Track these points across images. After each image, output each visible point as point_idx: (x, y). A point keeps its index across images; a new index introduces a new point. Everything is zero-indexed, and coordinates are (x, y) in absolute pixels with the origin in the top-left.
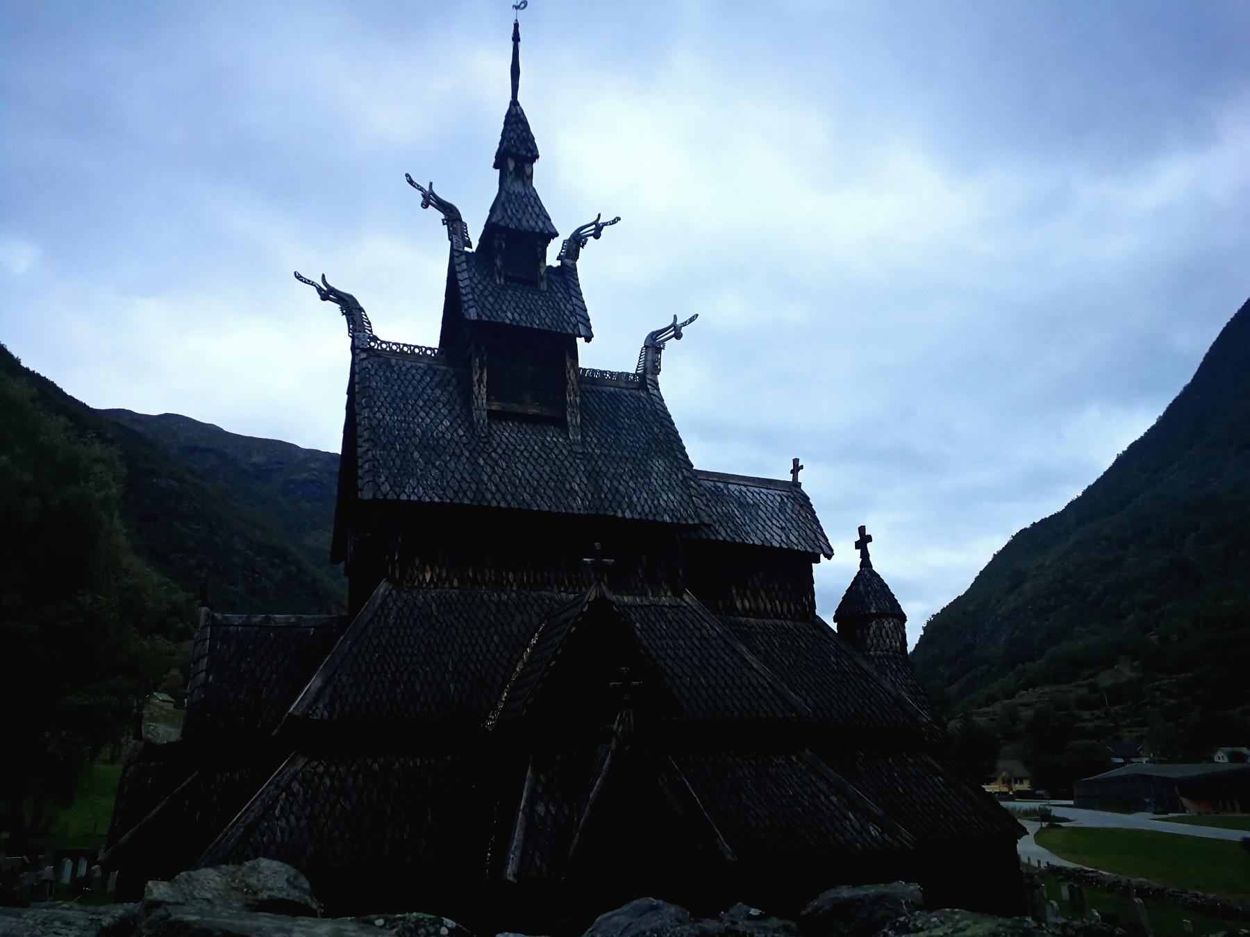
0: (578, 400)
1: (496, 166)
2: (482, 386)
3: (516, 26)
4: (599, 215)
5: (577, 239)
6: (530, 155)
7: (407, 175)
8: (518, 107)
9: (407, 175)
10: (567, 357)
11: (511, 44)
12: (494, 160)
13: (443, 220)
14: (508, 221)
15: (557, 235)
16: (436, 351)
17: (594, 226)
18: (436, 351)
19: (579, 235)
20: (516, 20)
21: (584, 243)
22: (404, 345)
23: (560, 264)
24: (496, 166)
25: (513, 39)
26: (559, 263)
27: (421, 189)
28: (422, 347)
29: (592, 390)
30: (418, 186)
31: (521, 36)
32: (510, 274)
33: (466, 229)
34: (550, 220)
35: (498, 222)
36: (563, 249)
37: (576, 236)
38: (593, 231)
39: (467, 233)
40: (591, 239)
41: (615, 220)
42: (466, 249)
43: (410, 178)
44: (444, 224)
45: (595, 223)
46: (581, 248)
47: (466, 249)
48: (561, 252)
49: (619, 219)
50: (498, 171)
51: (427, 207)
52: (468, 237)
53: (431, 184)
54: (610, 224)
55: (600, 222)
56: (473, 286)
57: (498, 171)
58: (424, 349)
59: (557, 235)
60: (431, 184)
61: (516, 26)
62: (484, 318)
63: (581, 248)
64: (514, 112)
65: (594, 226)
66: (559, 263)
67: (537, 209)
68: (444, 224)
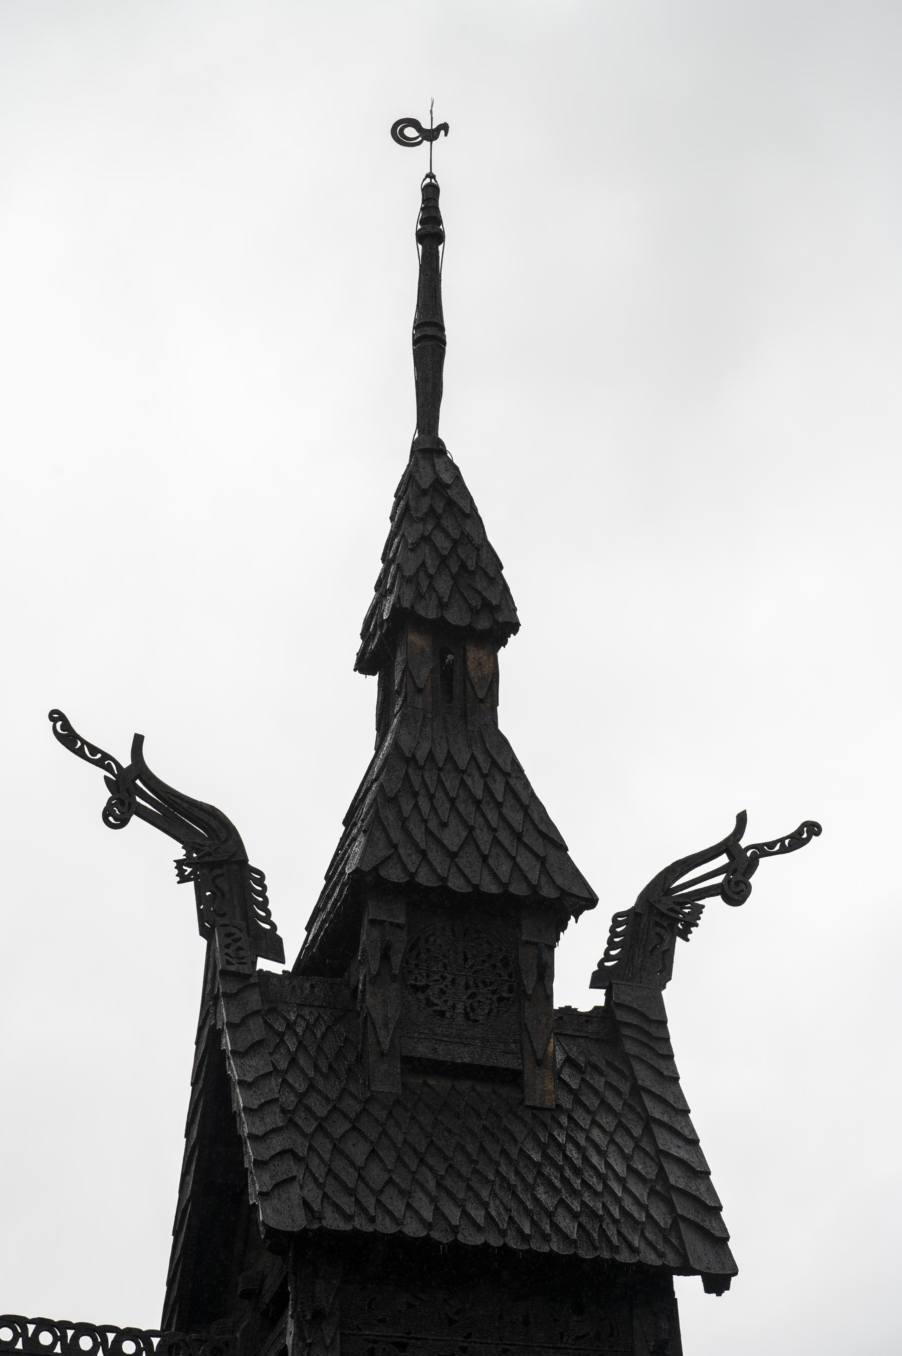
1: (364, 665)
3: (431, 193)
4: (742, 819)
6: (483, 624)
7: (56, 716)
8: (439, 462)
9: (56, 716)
11: (412, 253)
12: (357, 643)
13: (179, 864)
14: (412, 862)
15: (591, 901)
16: (156, 1341)
17: (723, 860)
18: (156, 1341)
19: (669, 892)
20: (431, 176)
21: (692, 921)
22: (43, 1324)
23: (601, 1002)
24: (364, 665)
25: (421, 237)
26: (599, 998)
27: (103, 760)
28: (106, 1329)
30: (94, 750)
31: (448, 226)
32: (422, 1050)
33: (263, 893)
35: (376, 869)
36: (611, 944)
38: (719, 879)
39: (264, 905)
40: (713, 905)
41: (799, 831)
42: (264, 964)
43: (66, 725)
44: (183, 879)
45: (729, 845)
46: (679, 940)
47: (264, 964)
48: (607, 957)
49: (812, 829)
50: (373, 681)
51: (122, 822)
52: (267, 919)
53: (138, 741)
54: (784, 850)
55: (744, 843)
56: (290, 1100)
57: (373, 681)
58: (111, 1336)
59: (591, 901)
60: (138, 741)
61: (431, 193)
62: (333, 1221)
63: (679, 940)
64: (425, 483)
65: (723, 860)
66: (599, 998)
67: (516, 818)
68: (183, 879)
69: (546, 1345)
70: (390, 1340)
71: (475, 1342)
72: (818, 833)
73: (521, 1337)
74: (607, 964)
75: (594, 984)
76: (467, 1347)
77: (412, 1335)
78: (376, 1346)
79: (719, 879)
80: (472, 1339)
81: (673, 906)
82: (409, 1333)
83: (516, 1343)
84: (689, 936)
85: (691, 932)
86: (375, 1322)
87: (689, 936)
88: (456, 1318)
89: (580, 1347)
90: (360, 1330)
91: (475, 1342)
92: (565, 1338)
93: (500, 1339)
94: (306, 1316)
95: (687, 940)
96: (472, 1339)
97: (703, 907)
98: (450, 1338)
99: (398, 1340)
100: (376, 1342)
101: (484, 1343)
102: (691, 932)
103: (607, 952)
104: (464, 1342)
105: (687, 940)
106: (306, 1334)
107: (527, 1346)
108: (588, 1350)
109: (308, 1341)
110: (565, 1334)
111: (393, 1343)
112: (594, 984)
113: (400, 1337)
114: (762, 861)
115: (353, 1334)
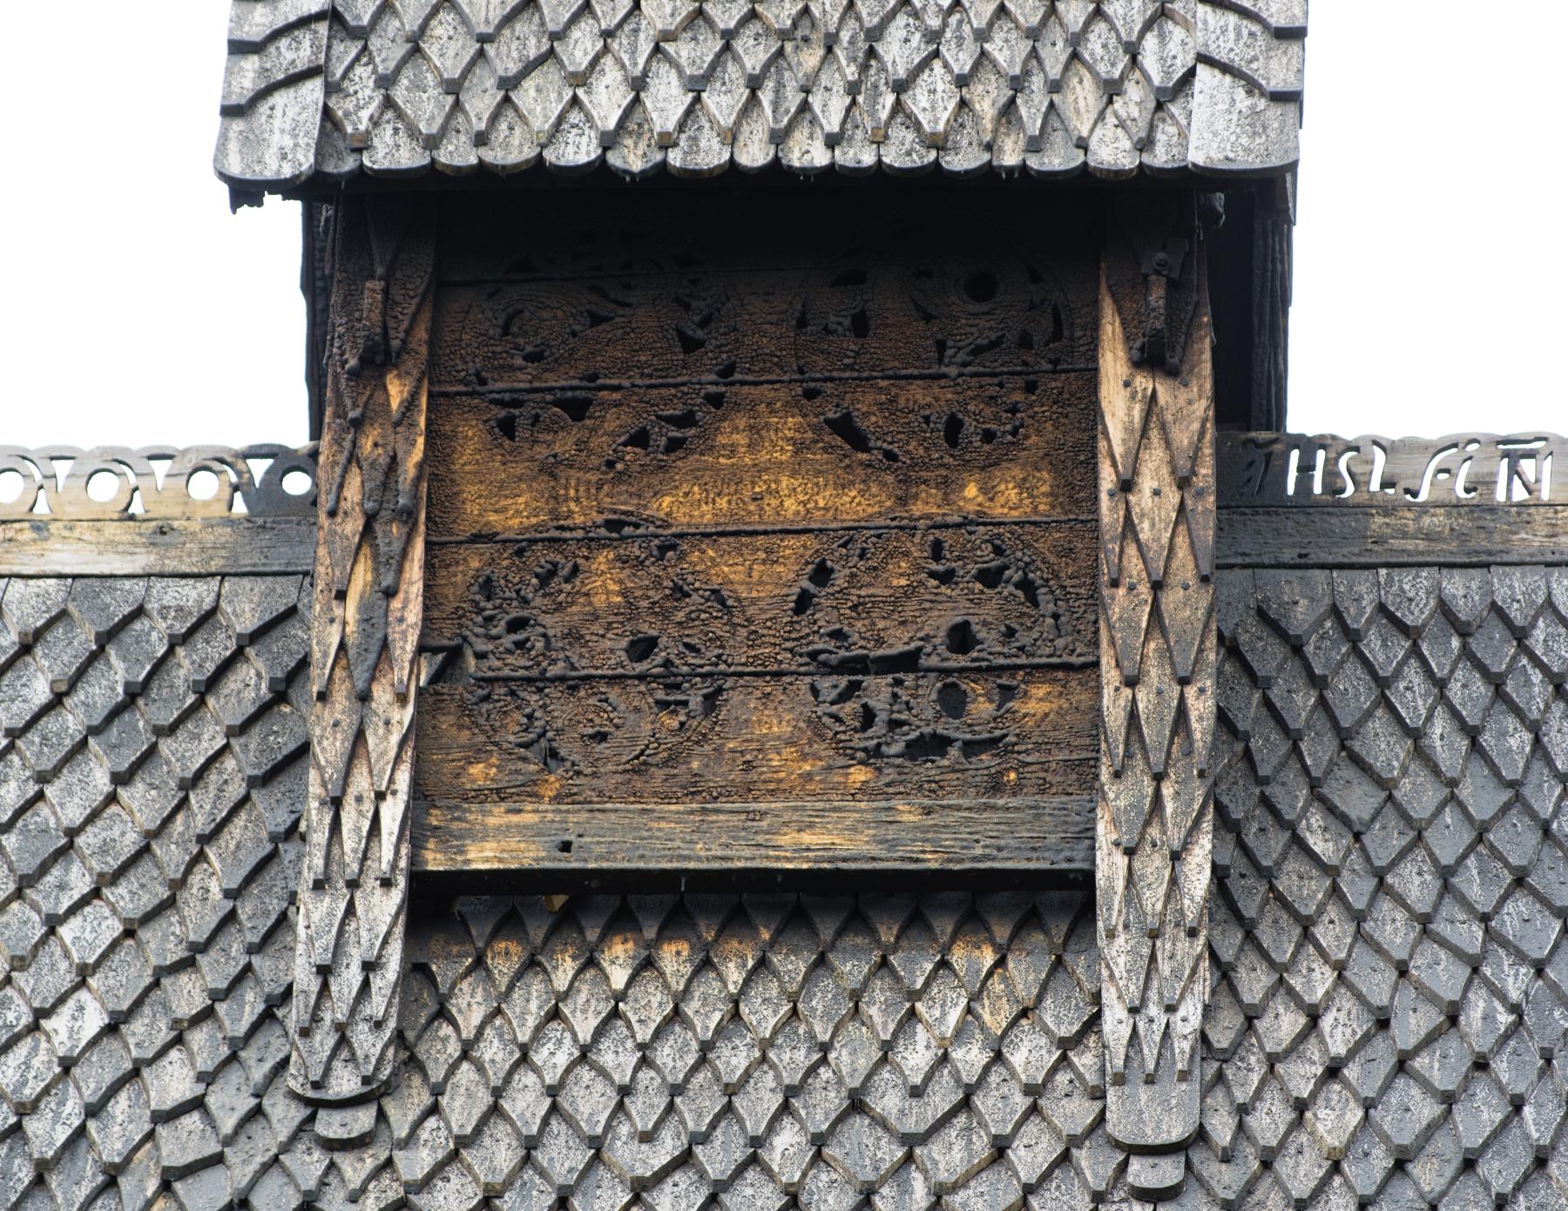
0: (1201, 708)
2: (382, 695)
10: (1113, 363)
29: (1445, 609)
69: (904, 372)
70: (549, 397)
71: (744, 383)
73: (846, 361)
76: (722, 395)
77: (600, 382)
78: (516, 412)
80: (737, 376)
82: (594, 377)
83: (835, 374)
86: (519, 362)
88: (700, 334)
89: (981, 369)
90: (483, 382)
91: (744, 383)
92: (950, 352)
93: (801, 371)
94: (346, 362)
96: (737, 376)
98: (686, 379)
99: (569, 394)
100: (517, 404)
101: (762, 383)
104: (717, 384)
106: (348, 402)
107: (861, 379)
108: (1002, 373)
109: (352, 415)
110: (950, 343)
111: (556, 403)
113: (572, 388)
115: (466, 394)
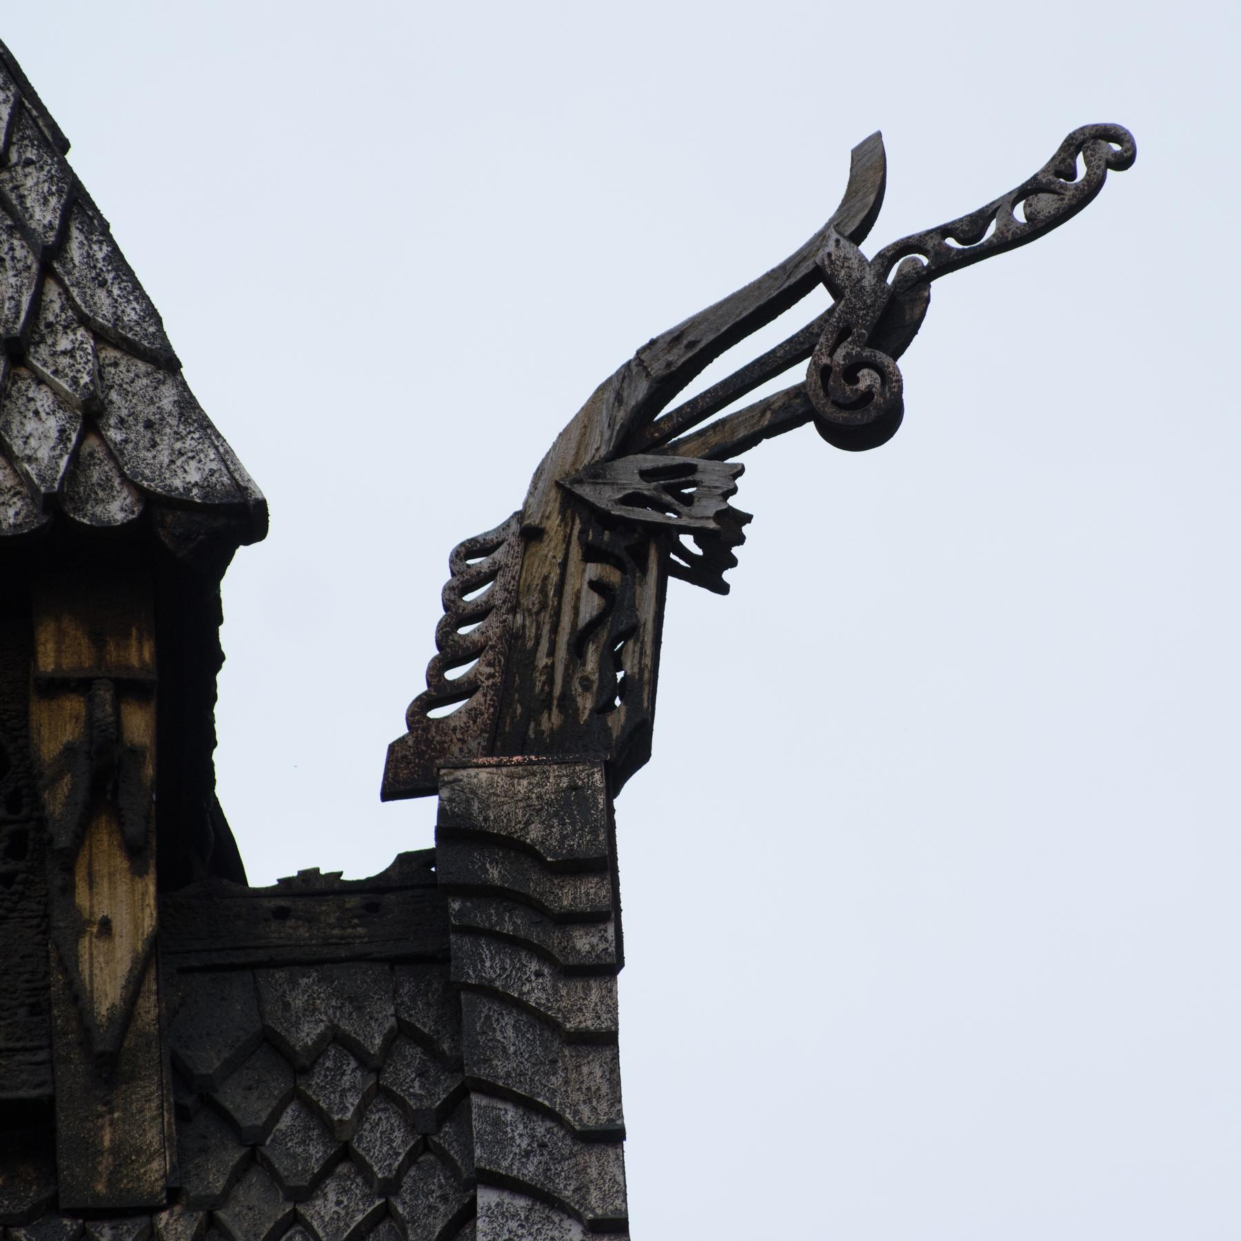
5: (604, 497)
17: (818, 301)
34: (167, 363)
37: (597, 473)
38: (796, 375)
41: (1061, 165)
48: (438, 692)
65: (818, 301)
72: (1124, 162)
74: (436, 713)
75: (391, 791)
79: (796, 375)
81: (647, 488)
84: (728, 575)
85: (733, 562)
87: (728, 575)
95: (723, 589)
97: (740, 471)
102: (733, 562)
103: (436, 671)
105: (723, 589)
112: (391, 791)
114: (940, 288)
